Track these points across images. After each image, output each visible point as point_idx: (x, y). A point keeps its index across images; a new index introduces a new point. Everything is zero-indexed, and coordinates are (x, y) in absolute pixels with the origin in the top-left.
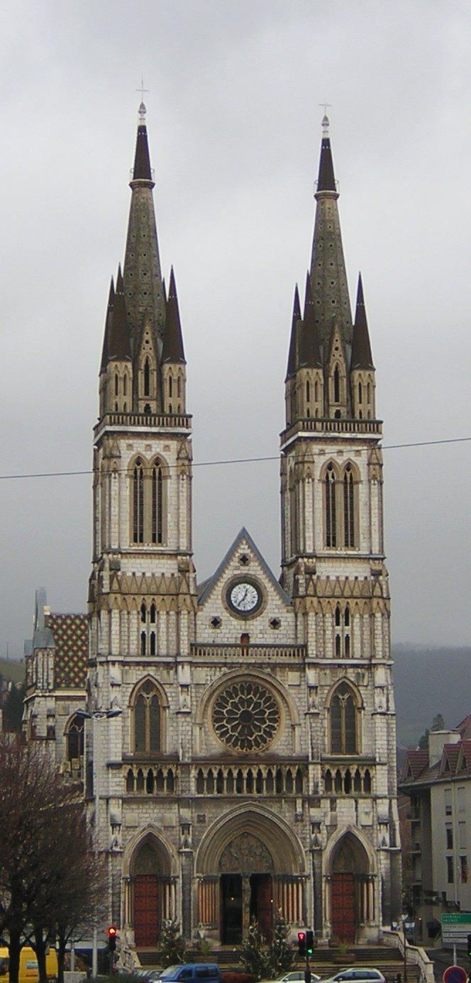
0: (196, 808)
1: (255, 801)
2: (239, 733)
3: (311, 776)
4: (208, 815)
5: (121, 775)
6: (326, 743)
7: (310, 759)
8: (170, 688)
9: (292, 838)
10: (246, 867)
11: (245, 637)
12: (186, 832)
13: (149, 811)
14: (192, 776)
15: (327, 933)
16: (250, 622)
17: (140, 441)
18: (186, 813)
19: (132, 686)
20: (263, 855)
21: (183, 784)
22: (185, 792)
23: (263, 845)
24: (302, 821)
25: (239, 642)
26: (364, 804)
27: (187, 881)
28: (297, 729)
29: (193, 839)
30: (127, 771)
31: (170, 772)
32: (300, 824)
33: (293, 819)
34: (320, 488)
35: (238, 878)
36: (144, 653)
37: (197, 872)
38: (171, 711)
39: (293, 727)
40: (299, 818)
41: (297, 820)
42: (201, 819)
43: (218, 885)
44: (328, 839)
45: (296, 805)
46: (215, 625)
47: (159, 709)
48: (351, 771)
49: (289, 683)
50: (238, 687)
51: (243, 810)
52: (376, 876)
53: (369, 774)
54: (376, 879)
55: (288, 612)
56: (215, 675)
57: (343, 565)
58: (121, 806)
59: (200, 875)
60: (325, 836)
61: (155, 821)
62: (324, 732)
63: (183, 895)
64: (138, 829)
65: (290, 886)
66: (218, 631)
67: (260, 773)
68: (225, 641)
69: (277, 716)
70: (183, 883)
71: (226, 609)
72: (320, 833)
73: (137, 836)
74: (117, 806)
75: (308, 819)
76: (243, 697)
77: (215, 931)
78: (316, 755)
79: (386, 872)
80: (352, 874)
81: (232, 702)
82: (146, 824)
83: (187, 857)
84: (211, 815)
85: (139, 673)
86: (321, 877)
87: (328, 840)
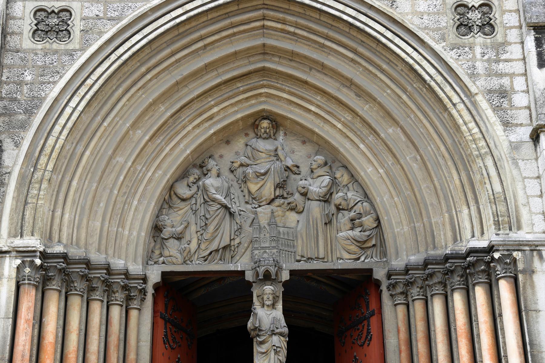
9: (448, 93)
10: (272, 240)
20: (338, 197)
23: (334, 160)
24: (488, 27)
32: (480, 39)
33: (447, 21)
35: (235, 291)
40: (475, 16)
43: (143, 321)
59: (33, 242)
65: (458, 300)
75: (512, 19)
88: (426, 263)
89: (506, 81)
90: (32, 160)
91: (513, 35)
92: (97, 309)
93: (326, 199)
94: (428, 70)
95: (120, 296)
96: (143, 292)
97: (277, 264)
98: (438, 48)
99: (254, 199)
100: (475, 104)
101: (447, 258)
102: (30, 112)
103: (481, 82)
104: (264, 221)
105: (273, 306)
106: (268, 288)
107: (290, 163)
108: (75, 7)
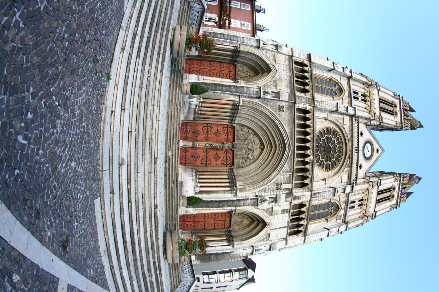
0: (288, 105)
1: (292, 152)
2: (321, 144)
3: (304, 193)
9: (266, 181)
12: (274, 95)
13: (285, 72)
15: (189, 211)
18: (285, 96)
20: (248, 160)
23: (255, 160)
24: (277, 189)
26: (284, 232)
27: (239, 91)
28: (324, 182)
30: (307, 64)
31: (308, 91)
32: (275, 187)
33: (279, 181)
39: (324, 180)
40: (279, 186)
41: (278, 184)
42: (281, 109)
44: (264, 210)
45: (287, 183)
48: (303, 221)
51: (286, 142)
52: (233, 246)
53: (300, 233)
54: (231, 247)
58: (287, 54)
59: (241, 104)
60: (266, 207)
61: (279, 75)
62: (320, 200)
63: (228, 86)
64: (274, 62)
72: (269, 203)
73: (269, 61)
74: (287, 52)
75: (278, 193)
77: (193, 116)
79: (236, 254)
80: (230, 226)
82: (277, 69)
83: (258, 91)
84: (284, 117)
87: (262, 209)
88: (234, 175)
89: (267, 191)
90: (257, 104)
91: (275, 193)
92: (229, 114)
93: (247, 158)
94: (270, 178)
95: (231, 118)
96: (231, 123)
97: (236, 148)
98: (274, 180)
99: (248, 144)
100: (263, 186)
101: (235, 179)
102: (265, 104)
103: (267, 187)
104: (244, 146)
105: (228, 147)
106: (231, 146)
107: (255, 151)
108: (284, 113)
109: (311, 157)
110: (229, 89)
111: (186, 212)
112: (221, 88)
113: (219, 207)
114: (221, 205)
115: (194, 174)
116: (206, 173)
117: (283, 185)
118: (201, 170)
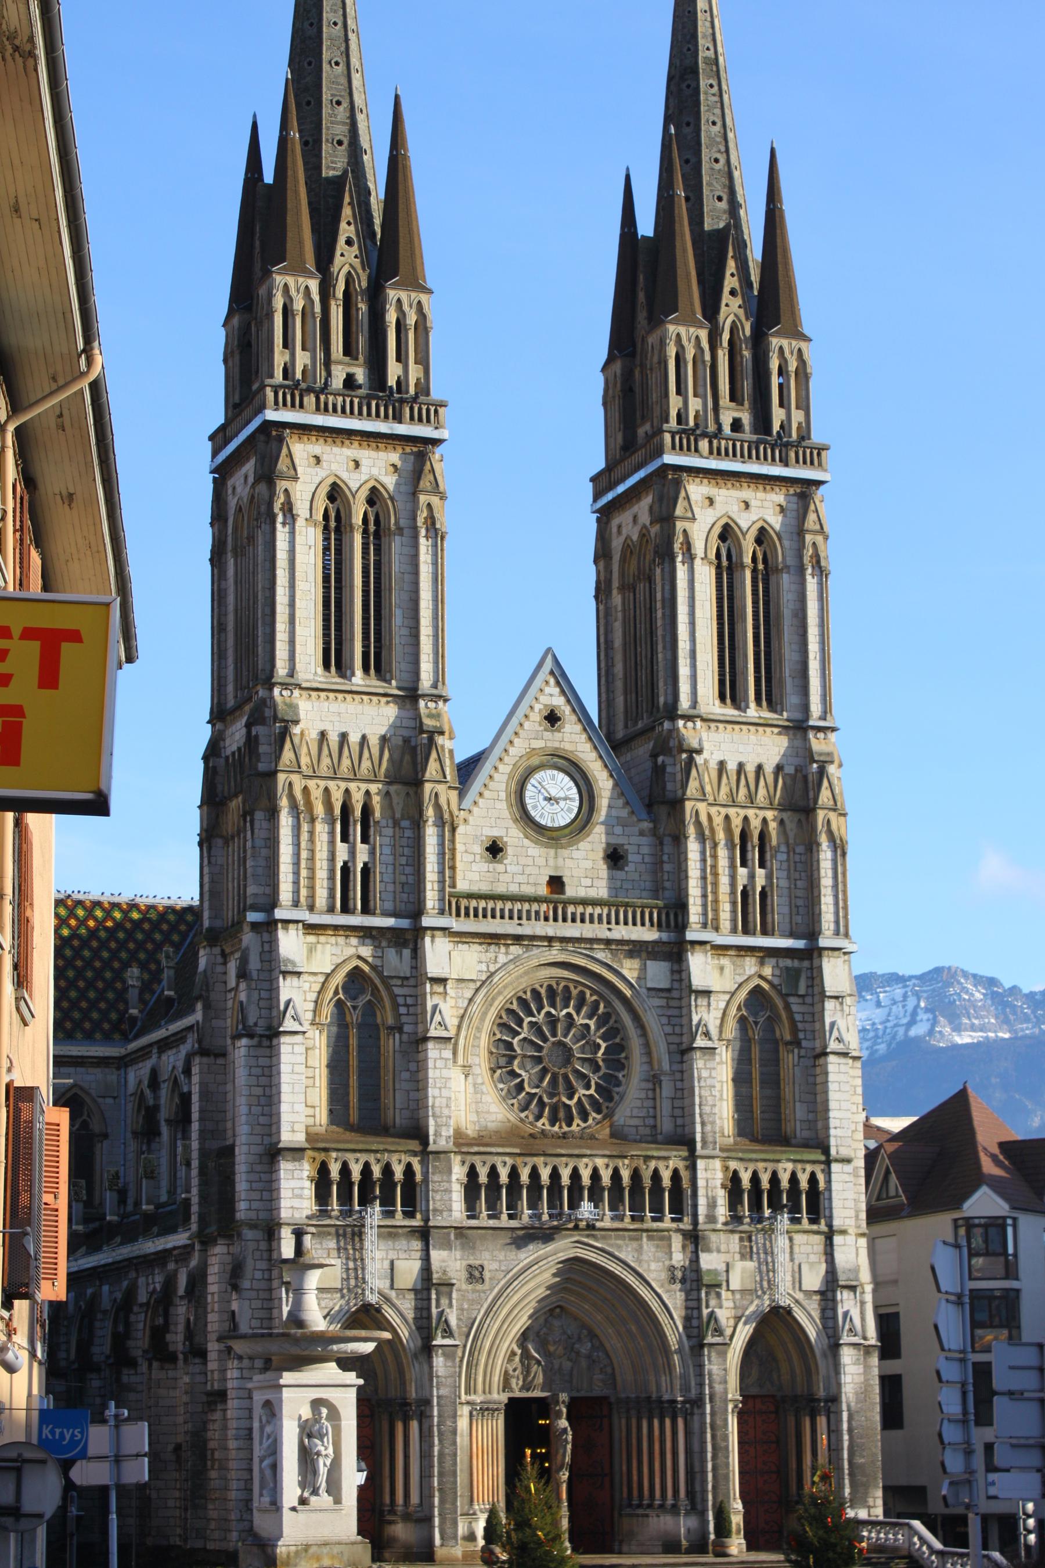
0: (463, 1248)
4: (490, 1266)
5: (306, 1174)
6: (725, 1115)
7: (699, 1145)
8: (402, 986)
11: (556, 883)
14: (454, 1177)
15: (738, 1525)
16: (564, 852)
17: (336, 450)
19: (321, 979)
21: (438, 1197)
22: (441, 1212)
25: (543, 890)
26: (808, 1245)
29: (459, 1319)
33: (664, 1275)
34: (705, 576)
36: (346, 909)
37: (468, 1392)
38: (405, 1037)
42: (476, 1275)
45: (670, 1246)
46: (494, 857)
47: (378, 1029)
49: (649, 985)
50: (543, 991)
55: (642, 833)
56: (496, 961)
57: (753, 738)
66: (500, 867)
67: (595, 1175)
68: (514, 889)
69: (623, 1055)
70: (439, 1416)
71: (515, 821)
72: (721, 1307)
76: (553, 1012)
78: (710, 1139)
79: (856, 1394)
80: (773, 1396)
81: (530, 1022)
84: (495, 1266)
85: (336, 950)
86: (726, 1401)
93: (589, 1357)
98: (659, 1291)
108: (486, 1263)
109: (600, 1162)
110: (449, 1435)
111: (738, 1532)
112: (448, 1458)
113: (727, 1447)
114: (723, 1444)
115: (640, 1511)
116: (635, 1478)
117: (674, 1263)
118: (625, 1490)
